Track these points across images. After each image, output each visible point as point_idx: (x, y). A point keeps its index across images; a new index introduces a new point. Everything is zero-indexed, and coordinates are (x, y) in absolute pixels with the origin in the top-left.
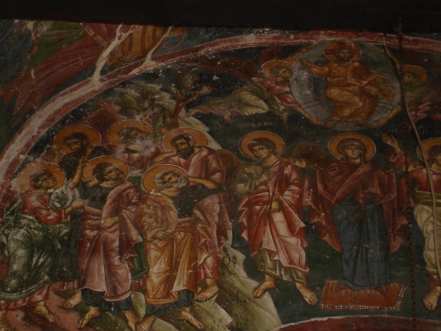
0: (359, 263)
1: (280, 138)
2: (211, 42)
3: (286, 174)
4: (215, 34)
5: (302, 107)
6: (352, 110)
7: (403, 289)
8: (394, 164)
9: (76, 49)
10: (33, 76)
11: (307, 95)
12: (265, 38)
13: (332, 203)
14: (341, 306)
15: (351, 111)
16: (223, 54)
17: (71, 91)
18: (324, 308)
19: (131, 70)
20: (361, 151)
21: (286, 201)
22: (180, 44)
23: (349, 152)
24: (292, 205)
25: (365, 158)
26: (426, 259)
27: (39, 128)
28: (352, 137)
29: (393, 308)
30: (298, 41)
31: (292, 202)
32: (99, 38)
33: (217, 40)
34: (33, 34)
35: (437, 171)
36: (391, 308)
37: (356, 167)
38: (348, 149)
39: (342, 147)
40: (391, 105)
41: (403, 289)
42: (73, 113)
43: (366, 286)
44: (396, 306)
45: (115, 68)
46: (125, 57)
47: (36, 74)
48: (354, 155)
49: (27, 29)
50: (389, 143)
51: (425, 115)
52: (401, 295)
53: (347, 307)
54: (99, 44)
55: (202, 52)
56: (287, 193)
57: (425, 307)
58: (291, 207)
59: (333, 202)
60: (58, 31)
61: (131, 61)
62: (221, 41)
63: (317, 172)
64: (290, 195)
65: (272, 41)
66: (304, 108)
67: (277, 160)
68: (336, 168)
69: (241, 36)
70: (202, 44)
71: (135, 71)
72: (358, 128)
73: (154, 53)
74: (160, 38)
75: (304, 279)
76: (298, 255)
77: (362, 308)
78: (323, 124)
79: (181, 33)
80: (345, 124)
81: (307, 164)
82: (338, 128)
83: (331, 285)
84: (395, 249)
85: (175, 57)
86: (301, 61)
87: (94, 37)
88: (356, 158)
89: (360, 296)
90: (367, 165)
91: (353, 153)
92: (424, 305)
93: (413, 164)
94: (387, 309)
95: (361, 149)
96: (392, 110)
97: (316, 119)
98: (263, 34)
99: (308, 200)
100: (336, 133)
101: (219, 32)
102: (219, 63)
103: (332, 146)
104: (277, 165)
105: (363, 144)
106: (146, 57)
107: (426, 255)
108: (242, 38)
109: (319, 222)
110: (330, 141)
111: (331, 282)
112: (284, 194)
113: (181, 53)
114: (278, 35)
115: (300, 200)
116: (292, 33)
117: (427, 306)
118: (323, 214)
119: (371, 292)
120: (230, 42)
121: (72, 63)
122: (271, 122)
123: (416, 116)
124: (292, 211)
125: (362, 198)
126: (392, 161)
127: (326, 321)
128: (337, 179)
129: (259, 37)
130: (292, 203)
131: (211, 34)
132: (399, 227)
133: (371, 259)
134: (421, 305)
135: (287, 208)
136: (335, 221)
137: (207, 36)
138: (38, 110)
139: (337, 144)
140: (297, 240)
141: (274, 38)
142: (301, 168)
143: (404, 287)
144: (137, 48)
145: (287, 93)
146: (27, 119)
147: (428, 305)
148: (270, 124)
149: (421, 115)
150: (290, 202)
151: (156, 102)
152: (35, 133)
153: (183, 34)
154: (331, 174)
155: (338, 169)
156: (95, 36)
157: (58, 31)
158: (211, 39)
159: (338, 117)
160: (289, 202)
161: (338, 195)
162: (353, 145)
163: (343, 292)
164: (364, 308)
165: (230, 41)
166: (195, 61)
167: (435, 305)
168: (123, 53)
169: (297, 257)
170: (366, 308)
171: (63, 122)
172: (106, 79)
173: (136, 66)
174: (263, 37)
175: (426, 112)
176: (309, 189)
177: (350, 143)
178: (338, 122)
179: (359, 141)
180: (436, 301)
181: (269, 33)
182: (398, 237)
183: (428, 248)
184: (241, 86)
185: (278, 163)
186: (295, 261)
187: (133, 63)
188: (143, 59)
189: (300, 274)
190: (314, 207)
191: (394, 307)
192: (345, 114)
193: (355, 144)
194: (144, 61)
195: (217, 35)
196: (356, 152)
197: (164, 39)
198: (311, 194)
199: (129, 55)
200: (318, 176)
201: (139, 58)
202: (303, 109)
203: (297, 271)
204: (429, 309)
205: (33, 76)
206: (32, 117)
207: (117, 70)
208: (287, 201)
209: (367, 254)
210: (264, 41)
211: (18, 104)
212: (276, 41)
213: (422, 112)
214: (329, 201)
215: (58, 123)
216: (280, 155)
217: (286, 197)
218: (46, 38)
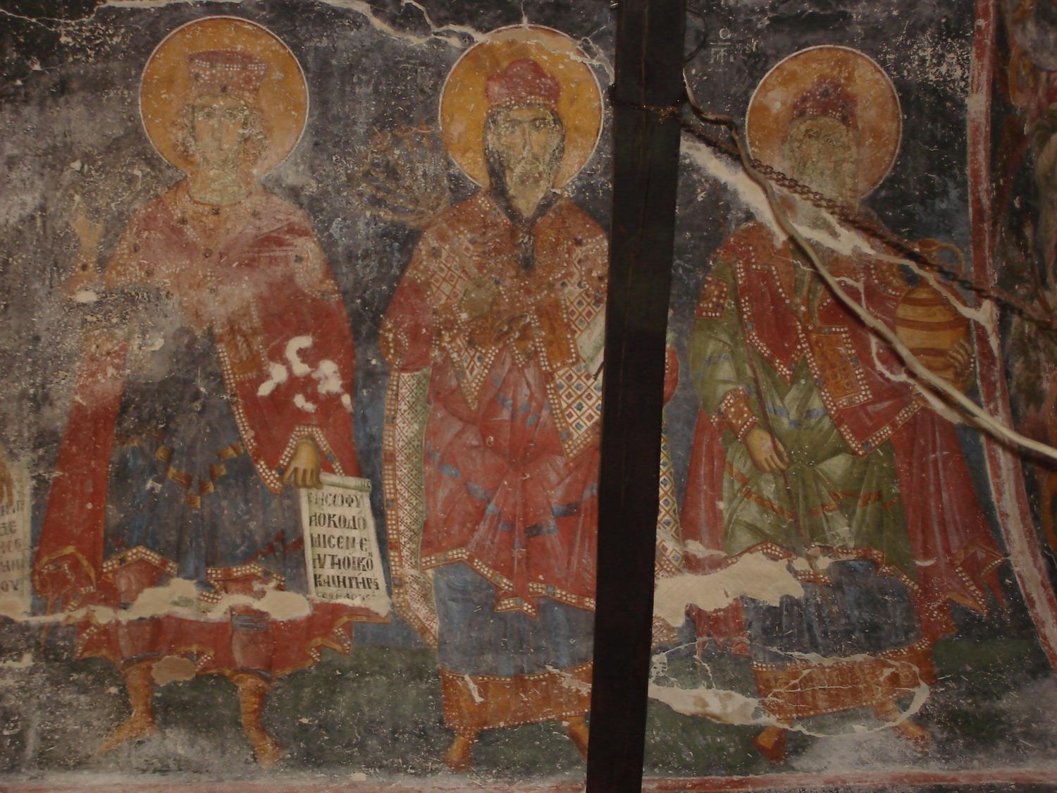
2: (969, 183)
4: (953, 177)
9: (910, 464)
10: (929, 563)
12: (979, 75)
16: (992, 168)
17: (997, 475)
19: (991, 351)
22: (958, 250)
27: (1035, 565)
30: (991, 9)
32: (902, 417)
33: (968, 171)
34: (844, 558)
42: (1029, 492)
45: (974, 386)
46: (957, 364)
47: (927, 555)
49: (828, 572)
54: (915, 417)
55: (986, 202)
60: (860, 502)
61: (970, 351)
62: (972, 161)
65: (986, 61)
69: (969, 124)
70: (970, 204)
71: (994, 342)
73: (965, 304)
74: (935, 292)
79: (934, 248)
85: (984, 259)
86: (1016, 22)
87: (896, 426)
98: (970, 80)
101: (951, 167)
102: (1001, 182)
106: (969, 320)
108: (973, 121)
113: (978, 247)
114: (974, 50)
116: (973, 23)
120: (978, 143)
121: (937, 473)
129: (975, 87)
131: (951, 184)
137: (954, 193)
138: (1007, 555)
141: (980, 57)
144: (944, 340)
145: (1048, 79)
146: (1015, 582)
151: (1033, 336)
152: (1040, 578)
153: (935, 245)
156: (894, 425)
157: (860, 502)
158: (962, 185)
165: (975, 144)
166: (994, 224)
168: (948, 366)
171: (1036, 518)
172: (991, 406)
173: (983, 339)
174: (975, 80)
181: (968, 69)
184: (1031, 163)
187: (976, 347)
188: (973, 326)
194: (976, 323)
195: (956, 171)
197: (939, 283)
199: (955, 354)
201: (968, 334)
205: (929, 563)
206: (1016, 569)
207: (978, 382)
210: (984, 77)
211: (969, 603)
212: (988, 53)
215: (1036, 527)
218: (864, 529)
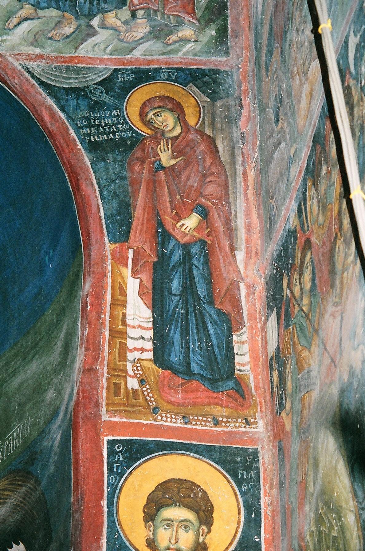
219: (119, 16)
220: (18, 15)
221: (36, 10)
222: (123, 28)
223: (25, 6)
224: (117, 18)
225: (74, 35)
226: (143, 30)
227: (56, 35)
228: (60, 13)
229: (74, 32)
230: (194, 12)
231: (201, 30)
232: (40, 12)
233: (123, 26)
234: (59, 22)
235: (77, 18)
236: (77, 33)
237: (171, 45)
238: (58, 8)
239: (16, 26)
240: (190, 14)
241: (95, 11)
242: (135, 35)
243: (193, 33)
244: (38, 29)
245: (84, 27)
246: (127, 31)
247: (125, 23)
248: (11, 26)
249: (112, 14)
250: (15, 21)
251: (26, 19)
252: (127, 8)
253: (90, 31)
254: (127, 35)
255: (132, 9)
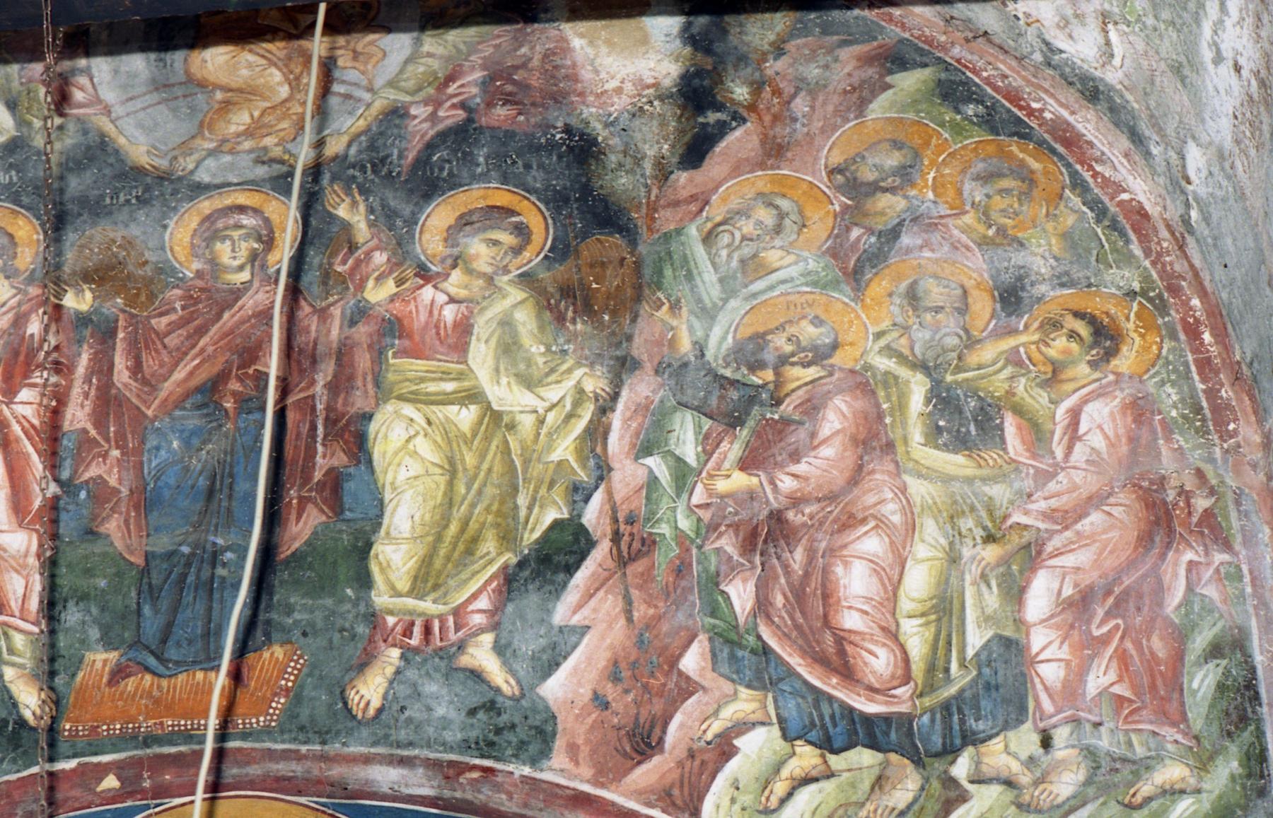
0: (188, 597)
1: (31, 222)
3: (32, 335)
5: (114, 115)
6: (256, 114)
7: (297, 662)
8: (342, 280)
11: (133, 75)
13: (145, 416)
14: (118, 726)
15: (252, 116)
18: (70, 735)
20: (256, 246)
21: (18, 422)
23: (223, 250)
24: (33, 432)
25: (264, 267)
26: (374, 568)
28: (241, 199)
29: (258, 722)
31: (36, 422)
35: (463, 293)
36: (254, 720)
37: (237, 293)
38: (223, 239)
39: (211, 231)
40: (370, 89)
41: (297, 662)
43: (194, 662)
44: (268, 714)
48: (234, 258)
50: (342, 212)
51: (461, 114)
52: (288, 680)
53: (133, 728)
56: (25, 394)
57: (350, 711)
58: (29, 438)
59: (150, 413)
63: (120, 323)
64: (31, 400)
66: (118, 118)
67: (14, 291)
68: (178, 305)
72: (261, 171)
75: (28, 655)
76: (23, 582)
77: (173, 726)
78: (163, 163)
80: (227, 158)
81: (94, 298)
82: (204, 177)
83: (99, 665)
84: (296, 545)
88: (241, 268)
89: (175, 691)
90: (268, 288)
91: (232, 254)
92: (345, 704)
93: (395, 274)
94: (244, 724)
95: (259, 239)
96: (369, 105)
97: (148, 152)
99: (77, 416)
100: (200, 189)
103: (178, 237)
104: (13, 308)
105: (267, 221)
107: (377, 556)
109: (100, 477)
110: (175, 219)
111: (104, 656)
112: (16, 400)
115: (56, 414)
117: (355, 708)
118: (116, 453)
119: (205, 678)
122: (13, 173)
123: (433, 117)
124: (30, 449)
125: (234, 394)
126: (339, 269)
127: (73, 770)
128: (172, 341)
130: (33, 426)
132: (318, 475)
133: (223, 579)
134: (340, 705)
135: (17, 440)
136: (146, 471)
139: (194, 225)
140: (30, 540)
142: (78, 313)
143: (301, 657)
147: (358, 704)
148: (11, 177)
149: (451, 116)
150: (29, 422)
154: (161, 323)
155: (183, 308)
159: (212, 140)
160: (26, 424)
161: (168, 386)
162: (238, 226)
163: (131, 684)
164: (179, 725)
167: (376, 703)
169: (20, 592)
170: (185, 725)
175: (463, 105)
176: (87, 380)
177: (231, 222)
178: (211, 153)
179: (256, 211)
180: (381, 691)
182: (311, 509)
183: (388, 533)
185: (13, 302)
186: (13, 604)
189: (19, 640)
190: (93, 432)
191: (262, 719)
192: (233, 129)
193: (245, 222)
196: (245, 248)
198: (93, 393)
200: (121, 335)
202: (112, 122)
203: (12, 633)
204: (360, 716)
208: (23, 420)
209: (214, 567)
213: (454, 106)
214: (138, 408)
216: (22, 278)
217: (20, 409)
219: (1013, 747)
220: (785, 773)
221: (823, 756)
222: (1025, 779)
223: (798, 750)
224: (1009, 754)
225: (916, 807)
226: (1072, 776)
227: (875, 811)
228: (880, 756)
229: (915, 800)
230: (1184, 718)
231: (1203, 763)
232: (835, 761)
233: (1026, 771)
234: (879, 778)
235: (918, 762)
236: (922, 799)
237: (1140, 806)
238: (874, 745)
239: (783, 801)
240: (1174, 724)
241: (958, 742)
242: (1055, 791)
243: (1187, 772)
244: (833, 804)
245: (936, 784)
246: (1037, 783)
247: (1031, 761)
248: (774, 802)
249: (996, 744)
250: (780, 788)
251: (807, 780)
252: (1028, 725)
253: (953, 794)
254: (1036, 793)
255: (1041, 725)
